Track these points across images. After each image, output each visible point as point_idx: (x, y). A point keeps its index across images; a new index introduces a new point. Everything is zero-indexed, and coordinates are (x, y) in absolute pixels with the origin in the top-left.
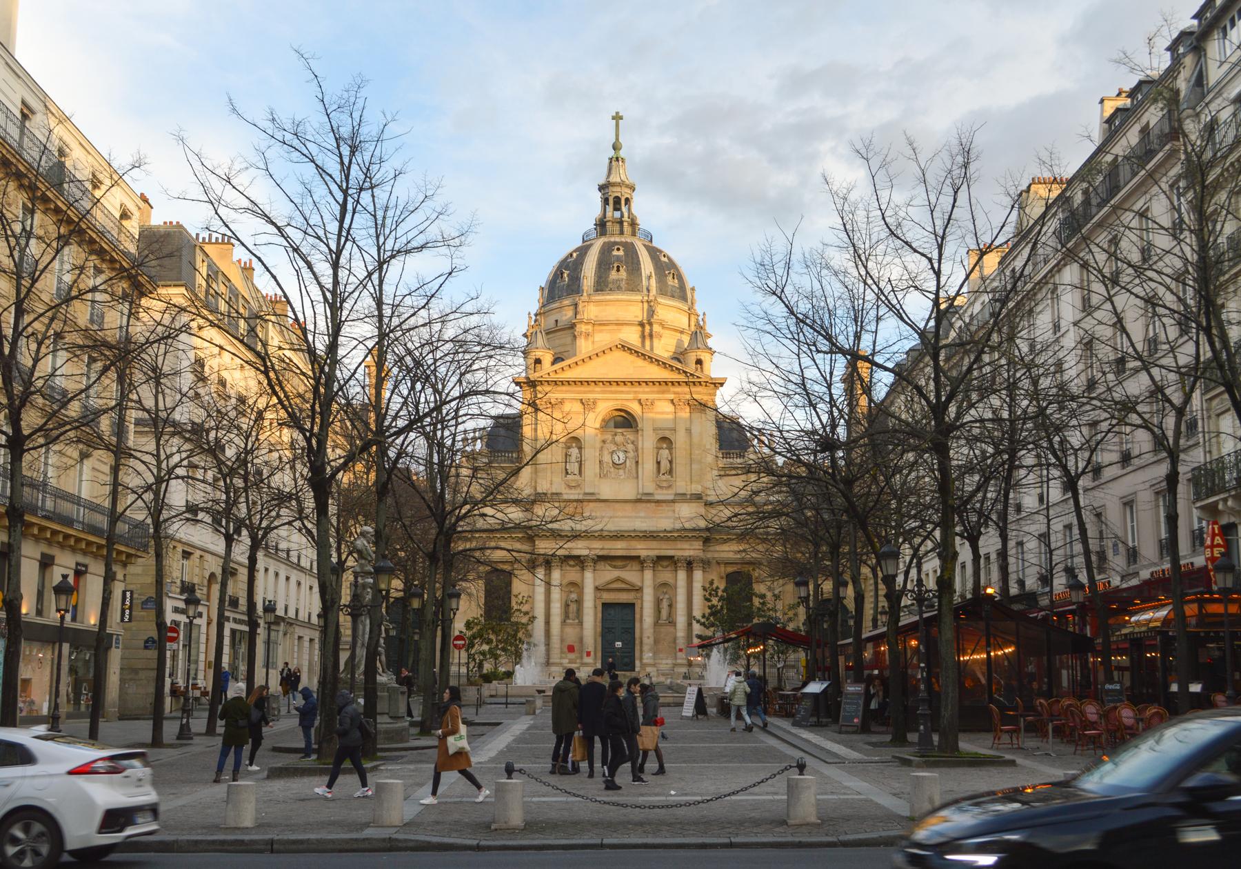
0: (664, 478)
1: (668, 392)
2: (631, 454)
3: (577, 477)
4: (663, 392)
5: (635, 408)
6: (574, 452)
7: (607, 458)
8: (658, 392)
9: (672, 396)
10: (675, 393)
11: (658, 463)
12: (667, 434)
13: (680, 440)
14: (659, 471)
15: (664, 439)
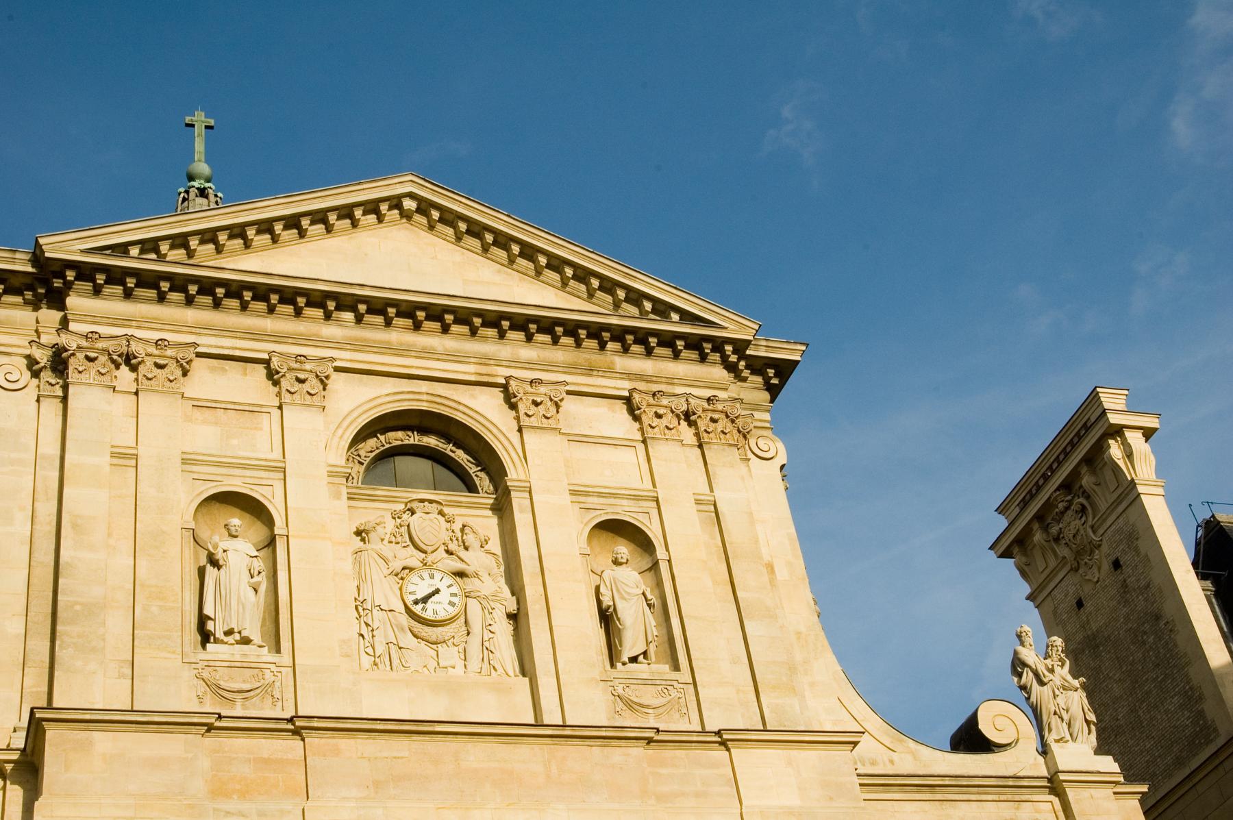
0: (641, 669)
1: (609, 371)
2: (492, 584)
3: (259, 653)
4: (590, 371)
5: (484, 411)
6: (240, 552)
7: (384, 593)
8: (572, 368)
9: (622, 387)
10: (630, 376)
11: (607, 618)
12: (624, 511)
13: (682, 536)
14: (613, 654)
15: (614, 528)
